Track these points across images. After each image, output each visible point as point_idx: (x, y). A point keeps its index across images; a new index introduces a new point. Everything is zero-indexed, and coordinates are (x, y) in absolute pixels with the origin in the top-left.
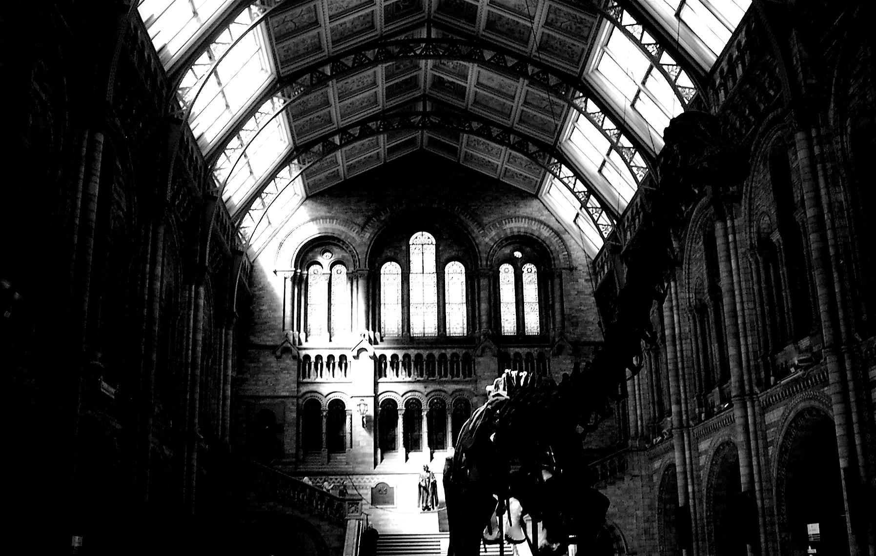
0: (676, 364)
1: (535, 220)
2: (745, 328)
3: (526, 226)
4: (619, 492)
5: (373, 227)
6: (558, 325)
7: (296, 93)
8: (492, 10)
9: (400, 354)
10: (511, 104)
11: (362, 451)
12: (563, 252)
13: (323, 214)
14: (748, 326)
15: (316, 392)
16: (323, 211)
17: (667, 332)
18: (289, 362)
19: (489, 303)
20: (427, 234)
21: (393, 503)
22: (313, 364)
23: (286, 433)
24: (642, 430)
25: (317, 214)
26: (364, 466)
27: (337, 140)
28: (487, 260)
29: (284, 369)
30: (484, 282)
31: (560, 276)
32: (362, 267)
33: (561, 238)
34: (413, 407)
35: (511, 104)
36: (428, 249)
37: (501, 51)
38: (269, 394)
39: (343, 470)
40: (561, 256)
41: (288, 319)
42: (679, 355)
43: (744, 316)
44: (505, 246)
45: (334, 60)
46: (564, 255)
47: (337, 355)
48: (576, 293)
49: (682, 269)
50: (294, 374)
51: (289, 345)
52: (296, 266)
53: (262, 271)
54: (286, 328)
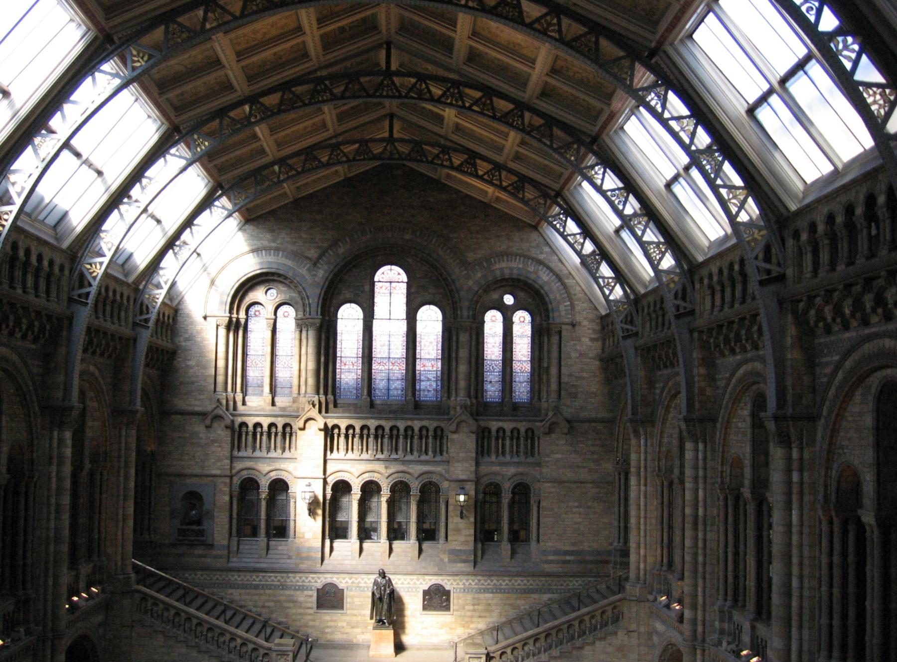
0: (695, 555)
1: (533, 259)
2: (800, 616)
3: (521, 266)
4: (610, 649)
5: (328, 263)
6: (554, 396)
7: (199, 149)
8: (474, 44)
9: (358, 425)
10: (503, 142)
11: (307, 545)
12: (565, 302)
13: (266, 243)
14: (806, 617)
15: (253, 469)
16: (266, 239)
17: (688, 511)
18: (221, 433)
19: (470, 363)
20: (397, 269)
21: (342, 608)
22: (250, 433)
23: (216, 520)
24: (645, 575)
25: (259, 244)
26: (309, 563)
27: (276, 168)
28: (469, 308)
29: (215, 441)
30: (464, 337)
31: (560, 333)
32: (313, 313)
33: (563, 284)
34: (370, 489)
35: (503, 142)
36: (397, 288)
37: (490, 92)
38: (196, 470)
39: (284, 566)
40: (562, 308)
41: (220, 379)
42: (700, 544)
43: (801, 597)
44: (495, 289)
45: (252, 99)
46: (565, 306)
47: (280, 422)
48: (578, 355)
49: (715, 427)
50: (227, 447)
51: (221, 412)
52: (231, 312)
53: (189, 316)
54: (218, 389)
